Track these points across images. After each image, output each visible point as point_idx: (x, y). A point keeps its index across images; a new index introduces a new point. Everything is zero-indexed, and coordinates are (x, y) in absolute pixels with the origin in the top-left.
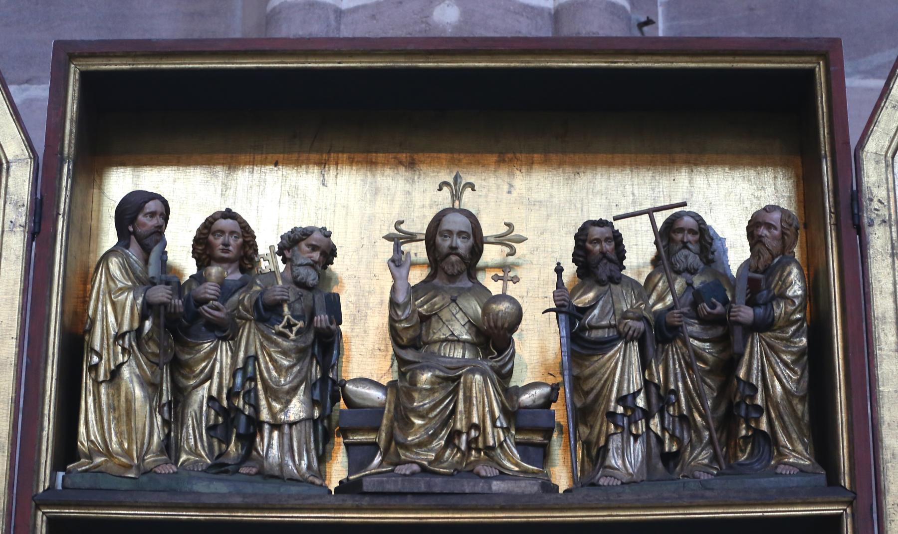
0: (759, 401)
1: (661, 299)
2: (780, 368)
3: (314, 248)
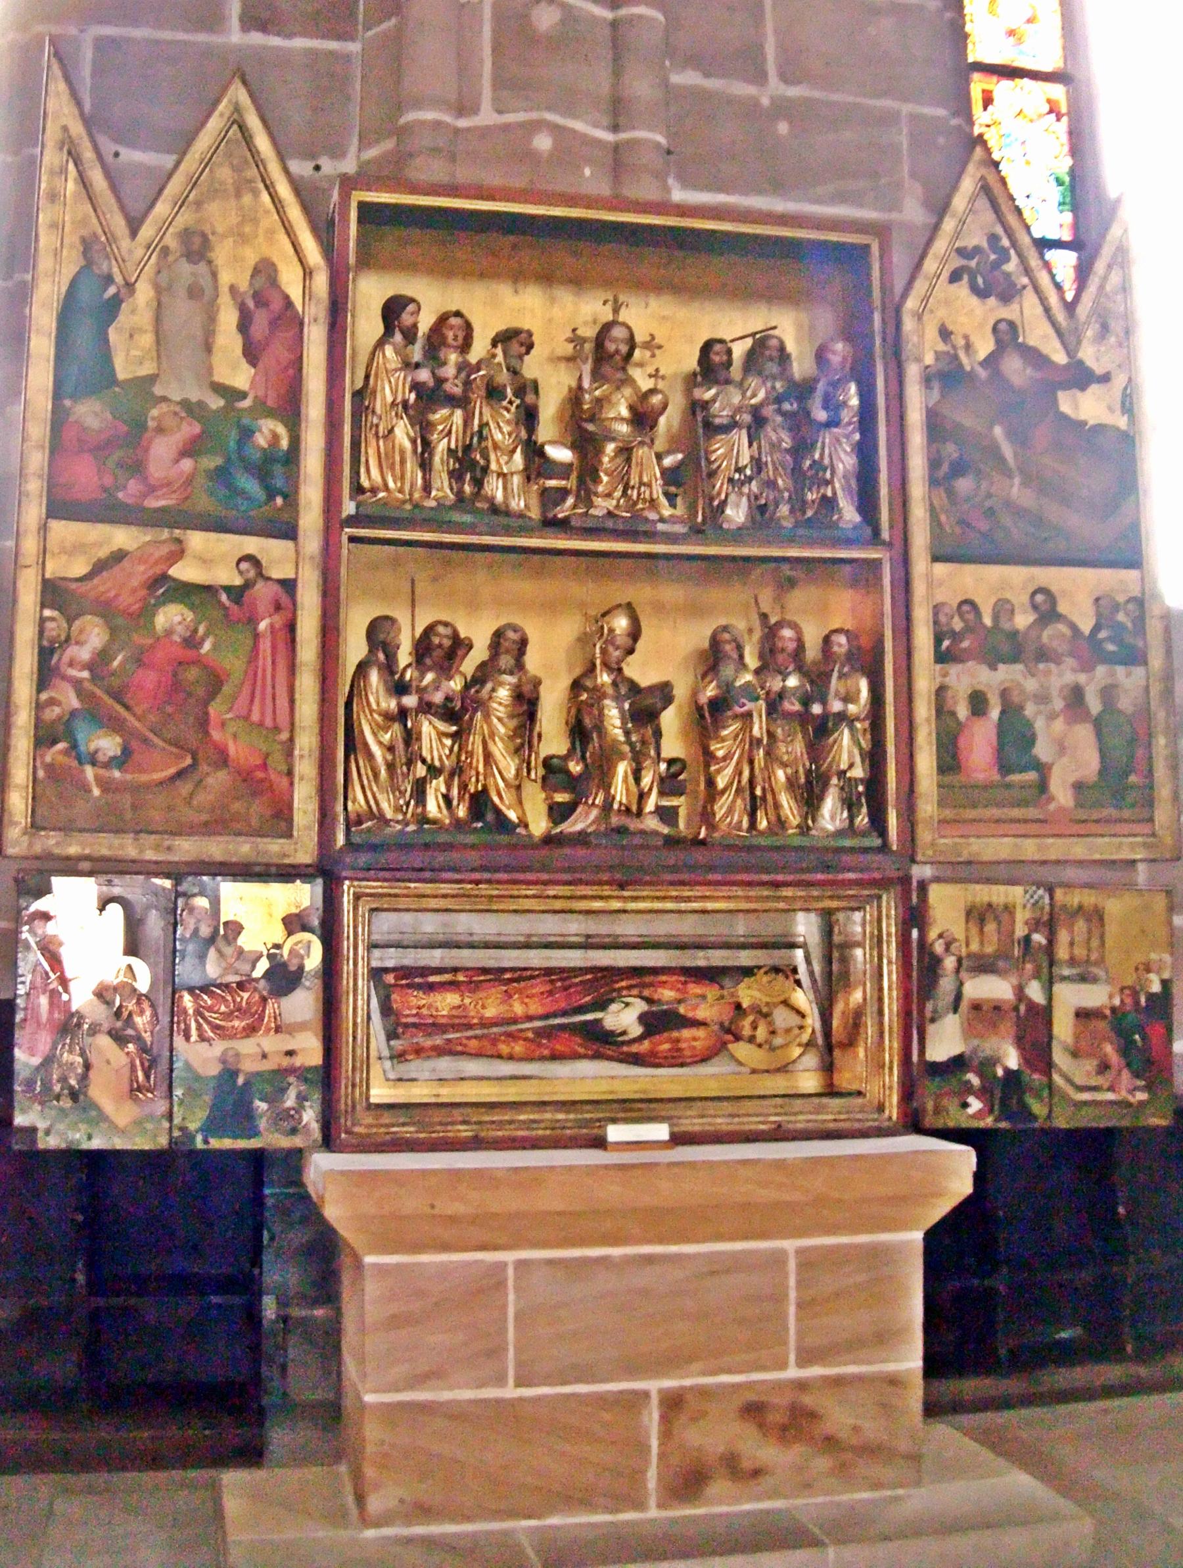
0: (828, 475)
1: (754, 395)
2: (843, 456)
3: (522, 345)
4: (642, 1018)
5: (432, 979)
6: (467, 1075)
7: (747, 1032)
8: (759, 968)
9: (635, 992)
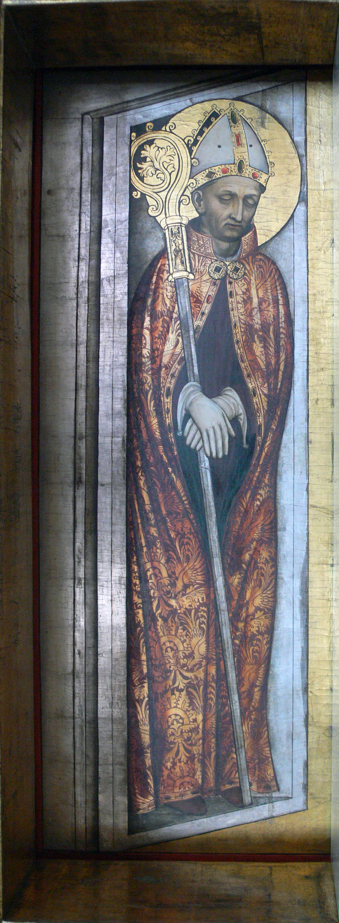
4: (212, 391)
5: (146, 739)
6: (298, 684)
7: (239, 212)
8: (132, 188)
9: (167, 402)
